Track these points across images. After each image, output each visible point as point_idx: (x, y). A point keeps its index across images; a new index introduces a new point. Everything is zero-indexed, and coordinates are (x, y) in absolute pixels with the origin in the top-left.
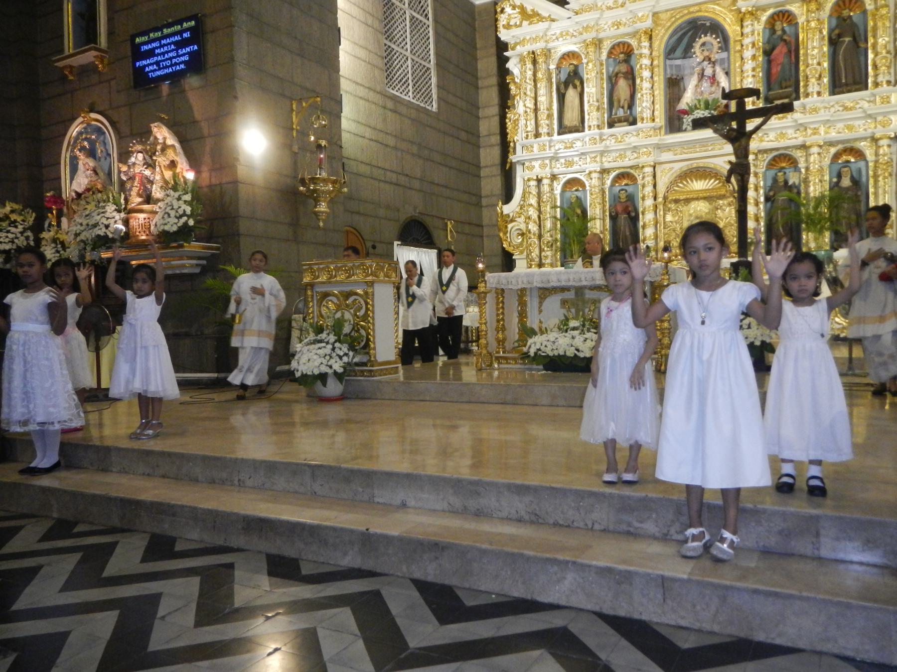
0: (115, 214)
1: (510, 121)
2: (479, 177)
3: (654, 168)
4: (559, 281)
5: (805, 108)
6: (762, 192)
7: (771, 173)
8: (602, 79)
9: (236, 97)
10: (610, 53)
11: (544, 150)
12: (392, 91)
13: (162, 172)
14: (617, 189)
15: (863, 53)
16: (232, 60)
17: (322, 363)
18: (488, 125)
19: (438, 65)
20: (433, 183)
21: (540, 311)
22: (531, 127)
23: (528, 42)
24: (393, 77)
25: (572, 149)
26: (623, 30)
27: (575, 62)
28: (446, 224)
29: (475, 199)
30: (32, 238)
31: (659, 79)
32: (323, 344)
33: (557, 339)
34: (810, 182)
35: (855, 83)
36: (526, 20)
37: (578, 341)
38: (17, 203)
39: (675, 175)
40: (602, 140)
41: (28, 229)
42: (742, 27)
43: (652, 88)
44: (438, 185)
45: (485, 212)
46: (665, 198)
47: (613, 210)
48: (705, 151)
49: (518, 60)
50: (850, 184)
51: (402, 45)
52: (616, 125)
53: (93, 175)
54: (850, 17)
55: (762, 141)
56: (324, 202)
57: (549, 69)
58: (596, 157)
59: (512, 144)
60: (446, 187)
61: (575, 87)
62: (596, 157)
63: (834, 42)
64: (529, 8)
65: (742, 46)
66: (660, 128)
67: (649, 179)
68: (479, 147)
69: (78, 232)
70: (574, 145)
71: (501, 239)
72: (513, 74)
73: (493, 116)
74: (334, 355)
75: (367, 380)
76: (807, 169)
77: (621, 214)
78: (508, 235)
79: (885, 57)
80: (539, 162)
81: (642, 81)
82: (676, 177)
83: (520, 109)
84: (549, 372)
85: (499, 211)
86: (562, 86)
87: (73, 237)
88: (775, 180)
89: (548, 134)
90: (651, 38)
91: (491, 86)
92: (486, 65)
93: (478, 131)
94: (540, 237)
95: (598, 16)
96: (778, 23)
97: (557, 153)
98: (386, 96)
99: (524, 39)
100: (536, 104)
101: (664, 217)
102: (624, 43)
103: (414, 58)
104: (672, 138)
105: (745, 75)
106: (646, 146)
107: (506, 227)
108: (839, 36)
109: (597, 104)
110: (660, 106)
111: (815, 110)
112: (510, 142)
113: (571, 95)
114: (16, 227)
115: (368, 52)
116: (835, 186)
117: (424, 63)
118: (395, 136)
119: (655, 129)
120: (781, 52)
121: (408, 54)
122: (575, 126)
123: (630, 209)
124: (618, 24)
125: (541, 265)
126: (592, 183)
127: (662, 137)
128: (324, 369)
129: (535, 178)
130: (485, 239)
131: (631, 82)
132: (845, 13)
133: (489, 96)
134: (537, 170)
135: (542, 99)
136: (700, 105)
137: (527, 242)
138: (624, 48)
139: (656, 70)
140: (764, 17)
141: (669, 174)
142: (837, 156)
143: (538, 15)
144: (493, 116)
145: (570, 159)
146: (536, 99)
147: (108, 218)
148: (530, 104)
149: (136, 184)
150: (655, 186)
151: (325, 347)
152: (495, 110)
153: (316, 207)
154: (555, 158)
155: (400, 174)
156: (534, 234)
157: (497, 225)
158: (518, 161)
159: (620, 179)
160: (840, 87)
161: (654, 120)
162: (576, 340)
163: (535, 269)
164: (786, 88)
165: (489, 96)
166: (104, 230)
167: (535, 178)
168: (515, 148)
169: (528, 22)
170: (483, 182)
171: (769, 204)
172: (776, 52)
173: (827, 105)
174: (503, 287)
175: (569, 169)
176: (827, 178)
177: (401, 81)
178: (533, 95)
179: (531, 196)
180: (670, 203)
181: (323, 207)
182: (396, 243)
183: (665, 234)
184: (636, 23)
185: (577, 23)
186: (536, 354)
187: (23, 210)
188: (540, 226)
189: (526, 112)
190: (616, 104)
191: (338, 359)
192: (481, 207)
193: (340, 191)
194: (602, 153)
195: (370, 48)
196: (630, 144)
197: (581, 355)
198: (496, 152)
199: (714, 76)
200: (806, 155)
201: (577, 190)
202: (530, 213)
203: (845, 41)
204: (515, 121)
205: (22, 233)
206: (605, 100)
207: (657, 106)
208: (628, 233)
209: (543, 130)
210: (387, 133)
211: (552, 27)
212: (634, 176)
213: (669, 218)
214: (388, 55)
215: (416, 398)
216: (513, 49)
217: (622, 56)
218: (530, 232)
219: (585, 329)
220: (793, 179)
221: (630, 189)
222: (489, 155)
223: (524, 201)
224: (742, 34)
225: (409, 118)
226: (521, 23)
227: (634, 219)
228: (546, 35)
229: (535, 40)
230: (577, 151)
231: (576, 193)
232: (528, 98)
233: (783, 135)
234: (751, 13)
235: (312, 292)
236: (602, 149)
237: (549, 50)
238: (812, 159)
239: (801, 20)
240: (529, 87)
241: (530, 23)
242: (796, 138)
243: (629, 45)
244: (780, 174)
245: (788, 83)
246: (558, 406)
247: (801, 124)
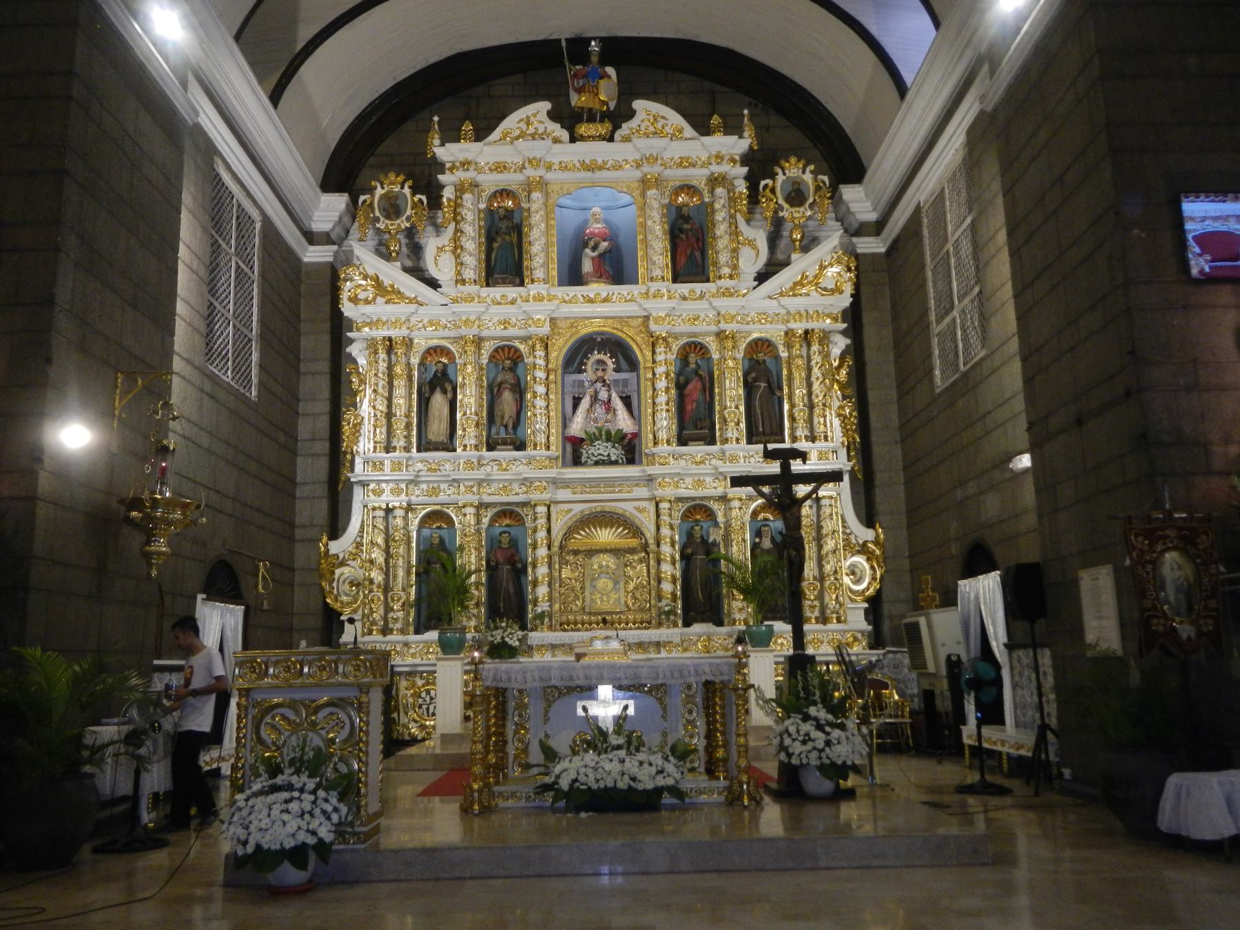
1: (349, 424)
2: (295, 498)
4: (586, 677)
5: (724, 453)
6: (677, 548)
7: (687, 526)
8: (481, 387)
9: (49, 360)
10: (492, 358)
11: (400, 470)
12: (210, 367)
14: (497, 530)
15: (776, 401)
16: (49, 301)
17: (299, 828)
18: (312, 424)
19: (262, 337)
20: (245, 504)
21: (546, 719)
22: (381, 435)
23: (384, 324)
24: (212, 348)
25: (439, 473)
26: (512, 332)
27: (444, 360)
28: (257, 569)
29: (286, 530)
31: (556, 398)
32: (296, 794)
33: (597, 763)
34: (732, 541)
35: (772, 434)
36: (383, 296)
37: (631, 765)
39: (574, 519)
40: (480, 465)
42: (654, 353)
43: (547, 407)
44: (251, 507)
45: (300, 550)
46: (561, 547)
48: (611, 492)
49: (365, 345)
50: (771, 546)
51: (225, 302)
52: (499, 447)
54: (764, 361)
55: (677, 487)
56: (164, 537)
57: (409, 364)
58: (472, 487)
59: (349, 457)
60: (258, 510)
61: (444, 392)
62: (472, 487)
63: (749, 387)
64: (387, 282)
65: (654, 374)
66: (557, 458)
67: (542, 521)
68: (296, 455)
70: (441, 468)
71: (322, 589)
72: (355, 361)
73: (320, 414)
74: (317, 811)
75: (354, 850)
76: (728, 525)
79: (801, 410)
80: (391, 485)
81: (535, 397)
82: (576, 522)
83: (365, 409)
84: (590, 814)
85: (323, 549)
86: (426, 389)
88: (690, 535)
89: (407, 449)
90: (546, 348)
91: (321, 373)
92: (314, 344)
93: (296, 430)
94: (386, 589)
95: (483, 310)
96: (692, 355)
97: (417, 476)
98: (205, 374)
99: (378, 320)
100: (389, 406)
101: (560, 572)
102: (510, 348)
103: (236, 323)
104: (573, 473)
105: (659, 408)
106: (540, 479)
107: (333, 573)
108: (755, 380)
109: (476, 418)
110: (557, 431)
111: (734, 459)
112: (345, 453)
113: (439, 401)
115: (189, 308)
116: (755, 547)
117: (246, 332)
118: (210, 433)
119: (550, 458)
120: (696, 389)
121: (230, 317)
122: (442, 443)
123: (516, 558)
124: (505, 323)
125: (385, 631)
126: (465, 521)
127: (562, 470)
128: (303, 837)
129: (384, 506)
130: (296, 588)
131: (517, 397)
132: (761, 356)
133: (315, 387)
134: (388, 498)
135: (400, 401)
136: (601, 435)
137: (364, 595)
138: (509, 353)
139: (552, 386)
140: (675, 347)
141: (567, 517)
142: (755, 514)
143: (399, 292)
144: (320, 414)
145: (435, 485)
146: (390, 399)
148: (382, 407)
150: (549, 531)
151: (299, 798)
152: (324, 407)
153: (148, 543)
154: (414, 482)
155: (211, 489)
156: (379, 586)
157: (318, 569)
158: (360, 481)
159: (500, 517)
160: (757, 436)
161: (548, 448)
162: (627, 764)
163: (376, 637)
164: (701, 429)
165: (315, 387)
168: (352, 462)
169: (384, 300)
171: (684, 562)
172: (690, 387)
173: (746, 454)
174: (501, 685)
175: (434, 498)
176: (748, 536)
177: (220, 354)
178: (386, 394)
179: (376, 531)
180: (568, 553)
181: (161, 545)
182: (200, 597)
183: (561, 595)
184: (530, 326)
185: (454, 313)
186: (571, 786)
188: (387, 574)
189: (375, 415)
190: (498, 420)
191: (323, 819)
192: (294, 541)
193: (195, 522)
194: (480, 483)
195: (192, 302)
196: (521, 474)
197: (640, 787)
198: (323, 465)
199: (609, 400)
200: (725, 509)
201: (438, 528)
202: (373, 556)
203: (760, 387)
204: (355, 426)
206: (485, 414)
207: (553, 431)
208: (512, 591)
209: (399, 442)
210: (201, 428)
211: (420, 312)
212: (518, 515)
213: (566, 573)
214: (209, 316)
215: (447, 876)
216: (358, 330)
217: (508, 362)
218: (371, 582)
219: (632, 748)
220: (715, 536)
221: (513, 531)
222: (311, 469)
223: (362, 537)
224: (654, 362)
225: (227, 408)
226: (374, 299)
227: (519, 569)
228: (409, 320)
229: (396, 324)
230: (449, 476)
231: (438, 531)
232: (379, 398)
233: (699, 483)
234: (664, 339)
235: (247, 700)
236: (483, 477)
237: (411, 340)
238: (735, 513)
239: (716, 356)
240: (381, 383)
241: (387, 302)
242: (715, 488)
243: (517, 350)
244: (697, 528)
245: (704, 424)
246: (680, 872)
247: (721, 473)
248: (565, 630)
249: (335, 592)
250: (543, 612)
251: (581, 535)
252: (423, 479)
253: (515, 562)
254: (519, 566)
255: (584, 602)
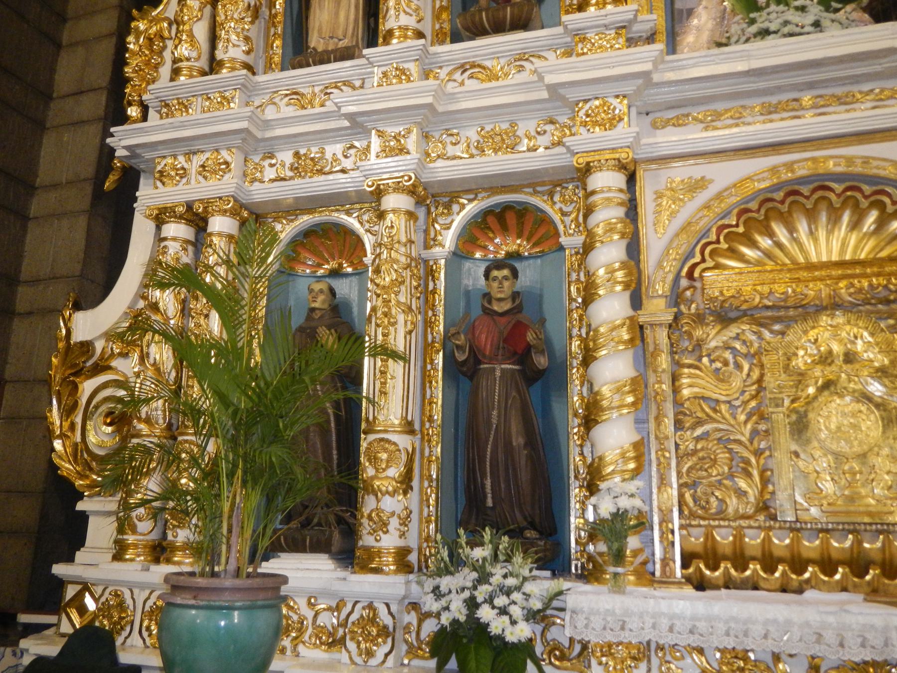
3: (631, 179)
47: (461, 340)
73: (98, 39)
77: (492, 359)
78: (79, 420)
101: (675, 378)
107: (75, 387)
123: (530, 337)
144: (98, 39)
150: (634, 249)
167: (181, 209)
170: (33, 234)
180: (699, 319)
201: (336, 273)
208: (518, 441)
212: (544, 220)
248: (701, 585)
249: (78, 438)
250: (619, 516)
251: (741, 258)
252: (279, 132)
253: (529, 348)
254: (541, 361)
255: (765, 481)
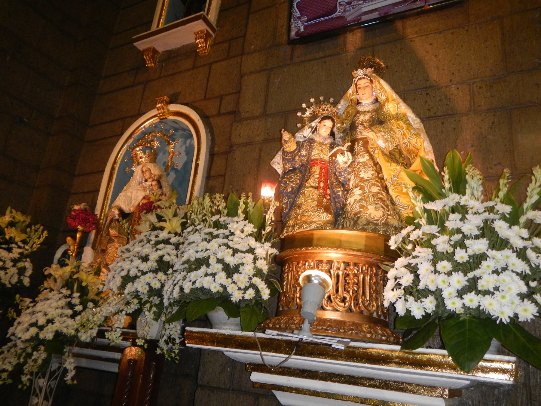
0: (252, 242)
13: (376, 164)
30: (29, 272)
38: (23, 213)
41: (27, 256)
53: (155, 188)
69: (132, 273)
87: (118, 281)
114: (9, 250)
147: (235, 251)
149: (312, 182)
166: (222, 277)
187: (29, 226)
205: (15, 261)
